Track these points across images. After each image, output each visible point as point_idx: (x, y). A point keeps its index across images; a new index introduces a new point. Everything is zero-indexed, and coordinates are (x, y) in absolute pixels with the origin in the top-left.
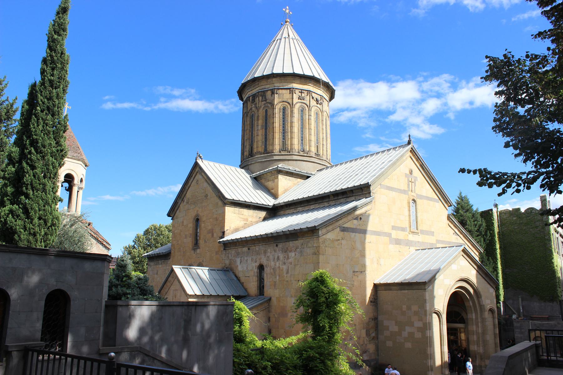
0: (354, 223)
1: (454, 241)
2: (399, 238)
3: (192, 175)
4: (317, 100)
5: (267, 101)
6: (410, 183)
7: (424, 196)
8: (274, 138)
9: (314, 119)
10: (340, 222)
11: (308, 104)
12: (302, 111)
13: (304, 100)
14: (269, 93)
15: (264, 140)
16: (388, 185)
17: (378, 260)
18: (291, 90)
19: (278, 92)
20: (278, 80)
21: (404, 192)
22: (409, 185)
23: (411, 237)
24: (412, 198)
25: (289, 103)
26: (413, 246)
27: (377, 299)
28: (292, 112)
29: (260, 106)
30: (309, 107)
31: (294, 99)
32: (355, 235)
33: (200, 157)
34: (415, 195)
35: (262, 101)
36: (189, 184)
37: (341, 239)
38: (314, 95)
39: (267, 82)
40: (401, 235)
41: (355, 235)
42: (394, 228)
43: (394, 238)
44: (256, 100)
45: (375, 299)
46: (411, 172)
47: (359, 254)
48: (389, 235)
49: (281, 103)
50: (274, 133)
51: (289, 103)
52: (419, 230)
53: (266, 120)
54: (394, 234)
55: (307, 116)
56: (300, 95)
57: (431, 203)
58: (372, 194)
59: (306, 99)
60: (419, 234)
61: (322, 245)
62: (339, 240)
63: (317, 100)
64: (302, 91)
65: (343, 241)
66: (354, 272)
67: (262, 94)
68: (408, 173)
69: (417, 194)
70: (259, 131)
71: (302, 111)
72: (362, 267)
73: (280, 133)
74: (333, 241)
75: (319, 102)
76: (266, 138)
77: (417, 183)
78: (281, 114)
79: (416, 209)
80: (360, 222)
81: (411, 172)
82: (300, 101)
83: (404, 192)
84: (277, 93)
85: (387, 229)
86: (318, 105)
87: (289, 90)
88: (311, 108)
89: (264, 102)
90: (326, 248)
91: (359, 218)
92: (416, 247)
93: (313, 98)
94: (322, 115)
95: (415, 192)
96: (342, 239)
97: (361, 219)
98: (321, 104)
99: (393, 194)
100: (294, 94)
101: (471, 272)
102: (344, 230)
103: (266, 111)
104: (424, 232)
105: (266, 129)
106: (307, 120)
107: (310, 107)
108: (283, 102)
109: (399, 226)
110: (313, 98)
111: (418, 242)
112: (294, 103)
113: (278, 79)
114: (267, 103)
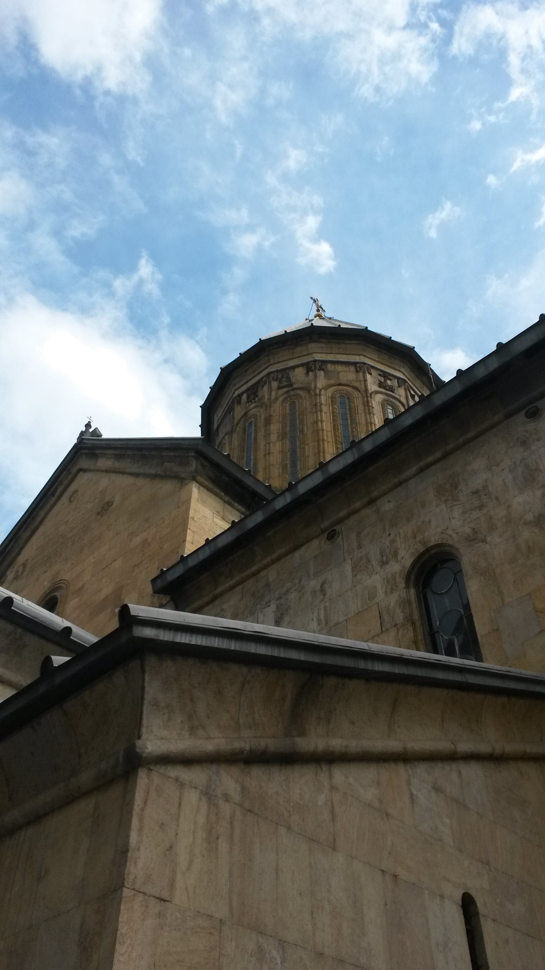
3: (56, 489)
8: (319, 453)
13: (393, 392)
15: (288, 462)
19: (324, 367)
20: (322, 347)
25: (354, 388)
29: (273, 397)
35: (279, 388)
36: (39, 519)
39: (293, 354)
44: (260, 394)
49: (335, 387)
50: (318, 441)
51: (354, 388)
64: (385, 375)
67: (279, 376)
70: (272, 445)
84: (320, 370)
100: (368, 376)
108: (340, 385)
113: (323, 345)
114: (294, 389)
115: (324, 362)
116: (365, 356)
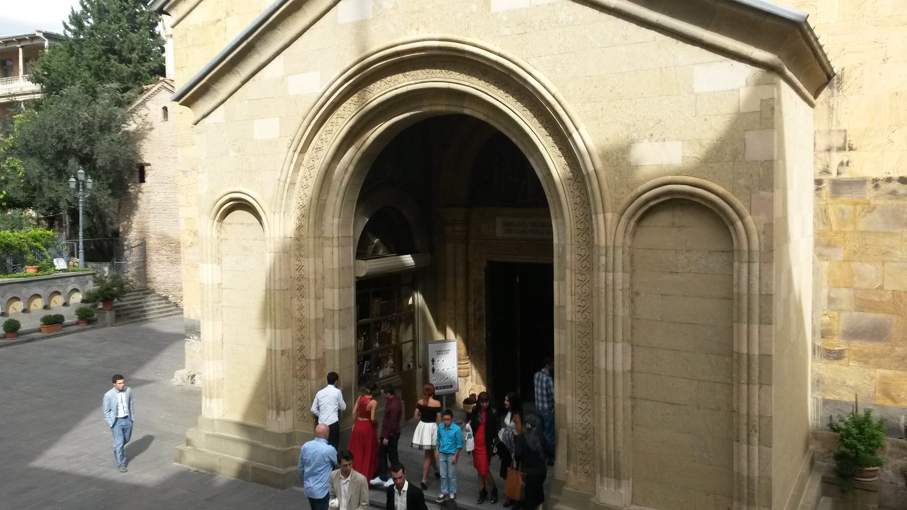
62: (220, 20)
96: (228, 14)
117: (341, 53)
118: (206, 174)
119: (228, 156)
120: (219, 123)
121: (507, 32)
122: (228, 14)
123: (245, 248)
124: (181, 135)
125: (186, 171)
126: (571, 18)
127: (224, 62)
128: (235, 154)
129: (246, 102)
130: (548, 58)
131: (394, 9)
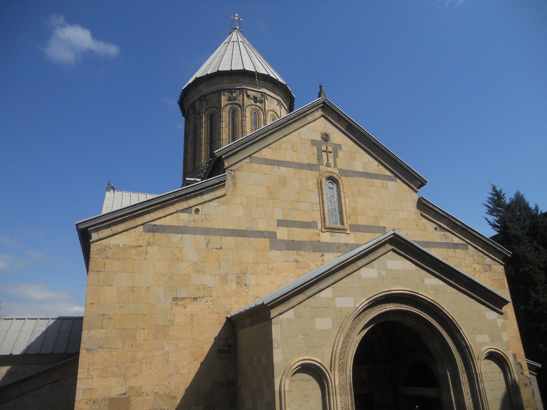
0: (181, 218)
1: (439, 241)
2: (296, 239)
4: (255, 99)
5: (197, 112)
6: (324, 154)
7: (358, 172)
9: (251, 120)
10: (147, 218)
11: (241, 103)
12: (233, 113)
14: (198, 102)
16: (269, 157)
17: (238, 277)
18: (219, 93)
21: (310, 167)
22: (322, 156)
23: (326, 237)
24: (328, 174)
26: (332, 251)
27: (236, 346)
28: (220, 116)
30: (242, 106)
31: (222, 102)
32: (182, 238)
33: (112, 187)
34: (337, 171)
35: (192, 114)
37: (147, 244)
38: (249, 92)
40: (300, 234)
41: (182, 238)
42: (281, 223)
43: (282, 240)
45: (229, 346)
46: (326, 138)
47: (192, 267)
48: (271, 236)
49: (209, 110)
52: (345, 225)
53: (195, 134)
54: (283, 233)
55: (240, 118)
56: (230, 96)
57: (377, 182)
58: (227, 172)
59: (238, 98)
60: (348, 232)
61: (96, 257)
62: (142, 246)
63: (255, 99)
65: (150, 249)
66: (175, 299)
68: (318, 138)
69: (341, 170)
71: (233, 113)
72: (198, 289)
73: (207, 144)
74: (125, 248)
75: (258, 99)
76: (195, 154)
77: (340, 154)
78: (208, 122)
79: (339, 192)
80: (196, 216)
81: (326, 138)
82: (230, 102)
83: (310, 167)
84: (204, 100)
85: (262, 226)
86: (258, 104)
87: (217, 94)
88: (245, 107)
89: (194, 115)
90: (107, 261)
91: (194, 208)
92: (339, 252)
93: (248, 96)
94: (265, 115)
95: (335, 166)
97: (197, 211)
98: (261, 102)
99: (283, 170)
101: (423, 281)
102: (155, 229)
103: (195, 124)
104: (355, 228)
105: (195, 144)
106: (240, 123)
107: (243, 106)
108: (211, 107)
109: (297, 220)
110: (248, 96)
111: (346, 244)
112: (223, 106)
113: (205, 84)
115: (205, 95)
116: (223, 83)
117: (364, 290)
118: (281, 349)
119: (298, 338)
120: (290, 319)
121: (431, 292)
122: (149, 244)
123: (306, 396)
124: (89, 320)
125: (91, 349)
126: (450, 291)
127: (303, 286)
128: (302, 337)
129: (309, 308)
130: (446, 303)
131: (386, 276)
